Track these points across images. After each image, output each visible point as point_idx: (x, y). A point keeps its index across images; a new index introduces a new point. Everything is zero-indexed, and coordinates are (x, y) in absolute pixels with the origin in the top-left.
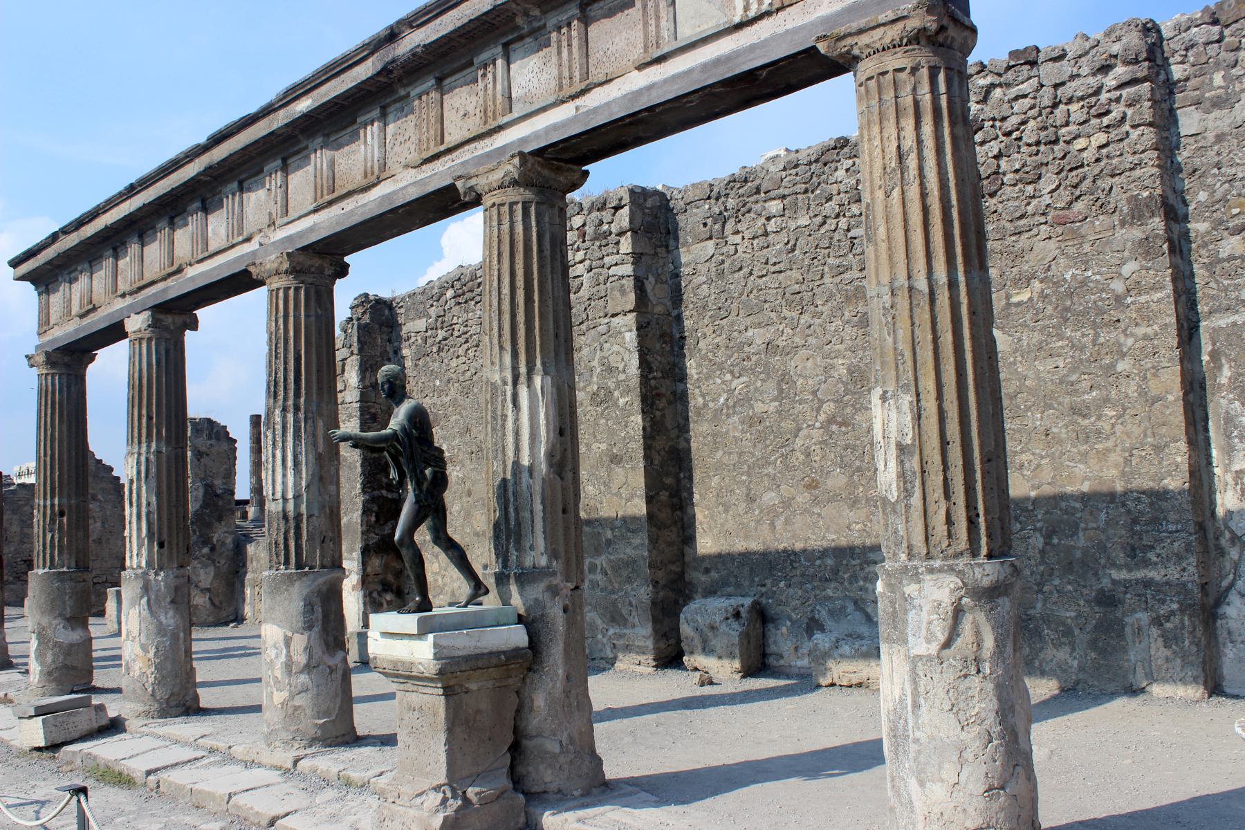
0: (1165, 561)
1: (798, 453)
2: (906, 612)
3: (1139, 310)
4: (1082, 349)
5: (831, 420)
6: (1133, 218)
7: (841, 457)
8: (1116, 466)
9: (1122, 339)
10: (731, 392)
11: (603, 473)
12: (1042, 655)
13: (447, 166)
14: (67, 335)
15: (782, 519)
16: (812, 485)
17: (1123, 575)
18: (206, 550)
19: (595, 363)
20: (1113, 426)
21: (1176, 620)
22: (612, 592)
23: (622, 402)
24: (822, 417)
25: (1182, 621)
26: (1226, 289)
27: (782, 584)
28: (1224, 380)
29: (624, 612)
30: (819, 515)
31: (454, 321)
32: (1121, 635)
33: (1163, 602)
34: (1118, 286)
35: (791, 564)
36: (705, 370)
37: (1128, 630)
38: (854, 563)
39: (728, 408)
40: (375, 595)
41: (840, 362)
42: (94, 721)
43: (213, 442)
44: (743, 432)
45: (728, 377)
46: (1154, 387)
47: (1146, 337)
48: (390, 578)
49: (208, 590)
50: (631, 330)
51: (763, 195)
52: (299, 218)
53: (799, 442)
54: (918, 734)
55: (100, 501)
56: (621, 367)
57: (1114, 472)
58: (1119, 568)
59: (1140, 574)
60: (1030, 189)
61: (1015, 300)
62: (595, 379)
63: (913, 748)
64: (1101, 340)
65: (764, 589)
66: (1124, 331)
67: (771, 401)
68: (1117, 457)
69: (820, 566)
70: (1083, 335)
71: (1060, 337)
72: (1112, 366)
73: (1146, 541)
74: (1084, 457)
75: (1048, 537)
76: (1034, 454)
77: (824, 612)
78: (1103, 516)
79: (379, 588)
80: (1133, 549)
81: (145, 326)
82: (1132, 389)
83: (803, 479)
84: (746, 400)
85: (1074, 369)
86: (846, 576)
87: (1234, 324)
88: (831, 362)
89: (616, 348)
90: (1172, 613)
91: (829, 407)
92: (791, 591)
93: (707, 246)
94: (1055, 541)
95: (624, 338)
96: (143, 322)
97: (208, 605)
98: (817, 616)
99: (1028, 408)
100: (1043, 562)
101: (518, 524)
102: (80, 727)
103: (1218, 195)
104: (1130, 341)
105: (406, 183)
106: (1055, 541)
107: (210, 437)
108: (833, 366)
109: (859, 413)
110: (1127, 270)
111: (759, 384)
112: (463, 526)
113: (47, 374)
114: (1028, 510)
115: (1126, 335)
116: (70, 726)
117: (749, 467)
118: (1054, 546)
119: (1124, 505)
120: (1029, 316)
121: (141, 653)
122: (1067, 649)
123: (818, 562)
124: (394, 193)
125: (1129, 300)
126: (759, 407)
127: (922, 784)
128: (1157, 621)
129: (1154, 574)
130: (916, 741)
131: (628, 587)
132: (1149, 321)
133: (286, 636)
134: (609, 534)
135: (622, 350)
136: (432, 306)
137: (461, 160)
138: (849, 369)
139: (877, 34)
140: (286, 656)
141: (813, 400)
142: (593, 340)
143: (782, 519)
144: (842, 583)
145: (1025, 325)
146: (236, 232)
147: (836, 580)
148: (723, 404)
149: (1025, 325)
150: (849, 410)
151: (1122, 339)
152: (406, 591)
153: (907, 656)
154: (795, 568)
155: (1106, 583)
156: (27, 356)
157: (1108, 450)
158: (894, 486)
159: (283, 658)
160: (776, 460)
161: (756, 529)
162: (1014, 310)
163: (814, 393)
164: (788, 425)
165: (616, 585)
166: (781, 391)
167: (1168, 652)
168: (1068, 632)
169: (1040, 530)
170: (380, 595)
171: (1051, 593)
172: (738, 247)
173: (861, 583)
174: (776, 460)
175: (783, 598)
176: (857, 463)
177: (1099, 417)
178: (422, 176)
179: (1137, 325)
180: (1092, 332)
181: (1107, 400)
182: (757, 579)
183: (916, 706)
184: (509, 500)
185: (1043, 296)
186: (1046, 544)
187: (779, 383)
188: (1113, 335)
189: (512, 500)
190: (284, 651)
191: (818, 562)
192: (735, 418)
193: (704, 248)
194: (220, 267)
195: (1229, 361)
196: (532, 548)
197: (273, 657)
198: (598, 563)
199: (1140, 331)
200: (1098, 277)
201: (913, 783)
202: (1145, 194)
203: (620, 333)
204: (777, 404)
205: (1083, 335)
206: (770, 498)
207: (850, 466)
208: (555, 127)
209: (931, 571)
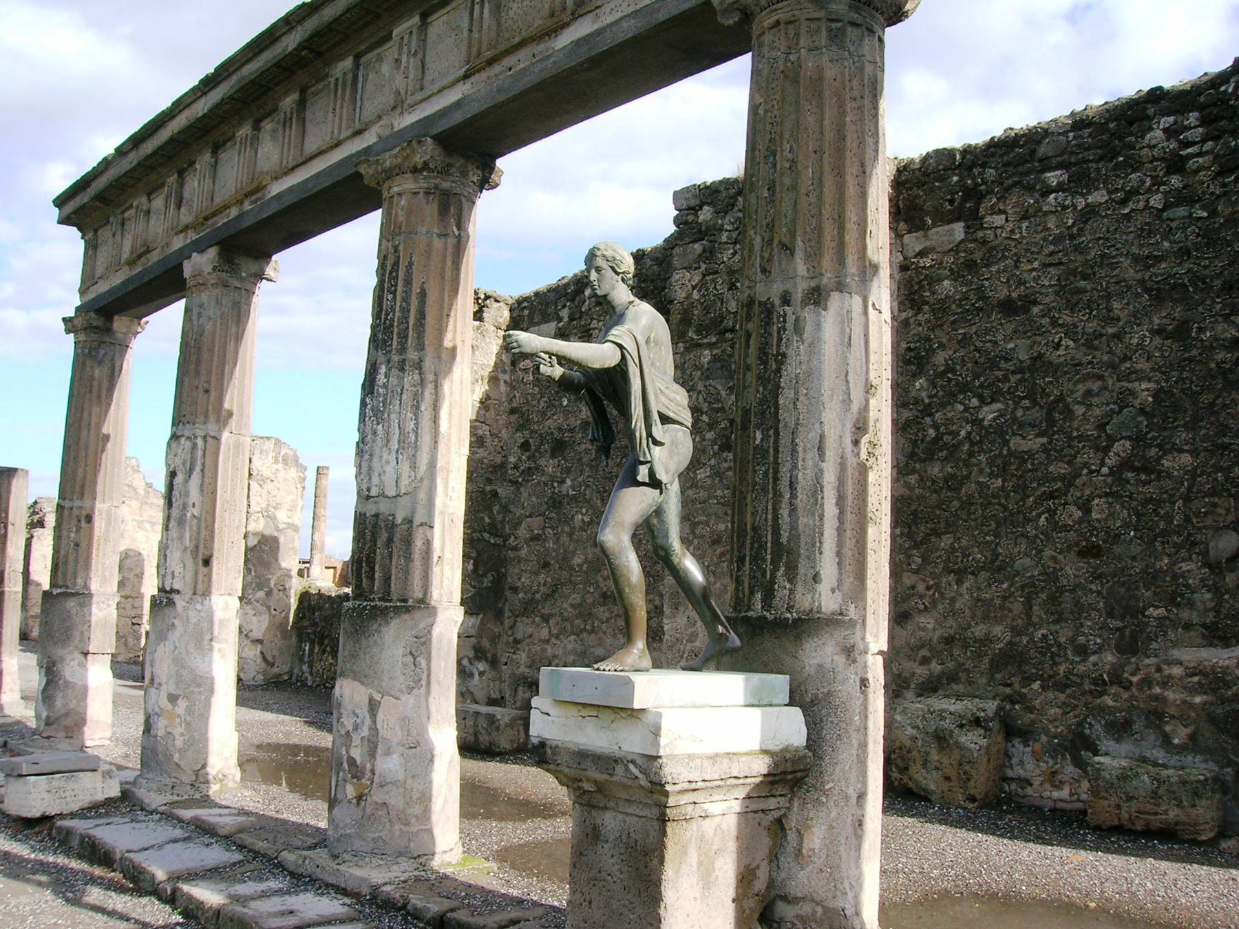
5: (1125, 464)
10: (978, 422)
14: (112, 291)
18: (261, 594)
24: (1111, 461)
31: (592, 326)
35: (1052, 658)
36: (941, 393)
38: (1147, 661)
39: (972, 444)
40: (465, 662)
41: (1143, 386)
42: (100, 790)
43: (280, 466)
45: (975, 402)
48: (486, 644)
49: (260, 641)
51: (1037, 164)
52: (440, 91)
55: (147, 531)
65: (1008, 690)
67: (1037, 436)
69: (1095, 664)
79: (471, 654)
84: (999, 432)
86: (1135, 679)
88: (1130, 386)
91: (1122, 447)
93: (953, 230)
97: (259, 660)
98: (1087, 732)
101: (795, 536)
102: (81, 797)
105: (620, 15)
107: (276, 461)
108: (1132, 393)
109: (1170, 457)
116: (67, 794)
117: (998, 524)
121: (170, 707)
124: (598, 32)
126: (1016, 443)
133: (371, 699)
136: (564, 306)
140: (370, 729)
141: (1099, 437)
146: (344, 125)
148: (965, 438)
150: (1153, 452)
152: (504, 660)
156: (64, 319)
159: (365, 732)
160: (1039, 515)
166: (1051, 422)
170: (471, 663)
172: (999, 231)
173: (1157, 690)
175: (1037, 703)
176: (1162, 525)
184: (781, 495)
187: (1049, 413)
189: (787, 495)
190: (368, 722)
192: (983, 458)
193: (951, 232)
194: (318, 175)
196: (816, 578)
197: (350, 728)
204: (1045, 440)
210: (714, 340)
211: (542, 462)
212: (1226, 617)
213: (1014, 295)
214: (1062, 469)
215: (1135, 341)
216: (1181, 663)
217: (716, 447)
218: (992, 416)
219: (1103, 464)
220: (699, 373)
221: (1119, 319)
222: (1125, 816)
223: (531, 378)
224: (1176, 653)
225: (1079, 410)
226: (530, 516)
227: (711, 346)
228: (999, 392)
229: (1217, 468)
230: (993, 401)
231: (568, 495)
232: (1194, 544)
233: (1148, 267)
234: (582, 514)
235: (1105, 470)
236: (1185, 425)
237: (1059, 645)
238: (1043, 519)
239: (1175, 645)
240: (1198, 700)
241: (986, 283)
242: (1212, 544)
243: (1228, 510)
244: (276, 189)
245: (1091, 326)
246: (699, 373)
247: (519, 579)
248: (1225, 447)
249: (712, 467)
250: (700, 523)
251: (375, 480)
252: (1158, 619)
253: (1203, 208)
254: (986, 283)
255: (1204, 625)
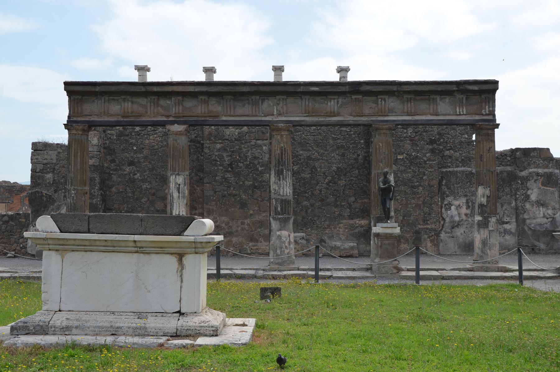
0: (432, 223)
1: (317, 191)
2: (489, 223)
3: (430, 165)
4: (415, 172)
5: (330, 182)
6: (430, 143)
7: (333, 193)
8: (422, 201)
9: (425, 171)
11: (250, 192)
12: (400, 246)
13: (366, 119)
15: (310, 210)
16: (322, 200)
17: (422, 227)
19: (249, 154)
20: (421, 191)
21: (433, 237)
22: (252, 231)
23: (260, 169)
24: (327, 181)
25: (435, 237)
26: (445, 162)
27: (309, 229)
28: (444, 184)
29: (257, 238)
30: (324, 209)
32: (420, 241)
33: (430, 233)
34: (425, 159)
35: (313, 223)
37: (422, 239)
44: (296, 182)
46: (432, 183)
47: (431, 172)
50: (266, 146)
53: (317, 187)
54: (490, 243)
56: (261, 157)
57: (421, 202)
58: (421, 225)
59: (425, 227)
60: (405, 131)
61: (398, 157)
62: (248, 160)
63: (489, 245)
64: (420, 171)
66: (426, 170)
67: (308, 174)
68: (421, 199)
70: (416, 169)
71: (410, 169)
72: (422, 177)
73: (428, 219)
74: (414, 198)
75: (404, 217)
76: (401, 197)
77: (326, 237)
78: (418, 213)
80: (424, 221)
81: (184, 130)
82: (427, 184)
83: (318, 198)
85: (413, 177)
87: (447, 171)
89: (258, 151)
90: (433, 235)
92: (313, 231)
94: (405, 218)
95: (263, 148)
96: (183, 129)
98: (323, 238)
99: (400, 185)
100: (402, 223)
103: (445, 141)
104: (427, 172)
105: (349, 119)
106: (405, 218)
110: (428, 155)
111: (304, 168)
112: (149, 207)
113: (81, 134)
114: (399, 210)
115: (426, 171)
117: (298, 193)
118: (405, 219)
119: (423, 210)
120: (402, 163)
122: (407, 244)
123: (323, 223)
124: (343, 120)
125: (428, 162)
126: (303, 175)
127: (490, 250)
128: (429, 237)
129: (429, 227)
130: (489, 244)
131: (259, 230)
132: (432, 168)
133: (289, 234)
134: (251, 212)
135: (261, 152)
137: (371, 119)
138: (337, 168)
139: (488, 126)
142: (248, 147)
143: (310, 210)
144: (331, 229)
145: (401, 165)
147: (329, 228)
149: (401, 165)
150: (336, 179)
151: (425, 171)
153: (488, 230)
154: (315, 225)
155: (417, 228)
156: (64, 124)
157: (420, 197)
158: (486, 202)
159: (288, 240)
160: (309, 192)
161: (300, 212)
162: (398, 160)
163: (324, 173)
164: (314, 182)
165: (254, 229)
167: (431, 245)
168: (407, 240)
169: (402, 215)
171: (404, 231)
174: (309, 192)
176: (338, 195)
177: (418, 190)
178: (356, 119)
179: (429, 169)
180: (418, 169)
181: (420, 185)
182: (299, 228)
183: (490, 238)
185: (406, 158)
186: (403, 219)
187: (312, 169)
188: (423, 170)
190: (288, 238)
191: (323, 223)
195: (445, 179)
197: (285, 240)
198: (246, 221)
199: (430, 170)
200: (420, 156)
201: (488, 250)
202: (434, 138)
203: (261, 146)
205: (416, 169)
206: (305, 203)
207: (336, 196)
208: (405, 120)
209: (493, 216)
210: (220, 141)
211: (124, 167)
212: (353, 214)
213: (302, 141)
214: (315, 182)
215: (332, 155)
216: (343, 223)
217: (223, 171)
218: (296, 168)
219: (325, 181)
220: (216, 150)
221: (329, 150)
222: (341, 254)
223: (115, 138)
224: (342, 221)
225: (319, 170)
226: (118, 185)
227: (220, 143)
228: (298, 163)
229: (351, 184)
230: (297, 165)
231: (138, 179)
232: (345, 199)
233: (336, 140)
234: (146, 185)
235: (325, 183)
236: (343, 175)
237: (315, 220)
238: (310, 193)
239: (342, 220)
240: (347, 230)
241: (295, 137)
242: (349, 199)
243: (353, 193)
244: (224, 118)
245: (322, 151)
246: (216, 150)
247: (113, 206)
248: (352, 180)
249: (221, 176)
250: (218, 191)
251: (285, 192)
252: (338, 214)
253: (349, 129)
254: (295, 137)
255: (348, 216)
